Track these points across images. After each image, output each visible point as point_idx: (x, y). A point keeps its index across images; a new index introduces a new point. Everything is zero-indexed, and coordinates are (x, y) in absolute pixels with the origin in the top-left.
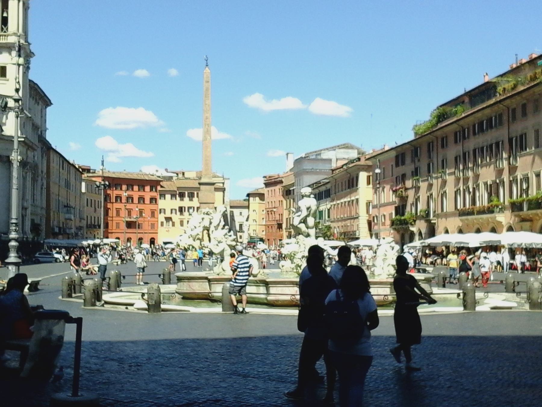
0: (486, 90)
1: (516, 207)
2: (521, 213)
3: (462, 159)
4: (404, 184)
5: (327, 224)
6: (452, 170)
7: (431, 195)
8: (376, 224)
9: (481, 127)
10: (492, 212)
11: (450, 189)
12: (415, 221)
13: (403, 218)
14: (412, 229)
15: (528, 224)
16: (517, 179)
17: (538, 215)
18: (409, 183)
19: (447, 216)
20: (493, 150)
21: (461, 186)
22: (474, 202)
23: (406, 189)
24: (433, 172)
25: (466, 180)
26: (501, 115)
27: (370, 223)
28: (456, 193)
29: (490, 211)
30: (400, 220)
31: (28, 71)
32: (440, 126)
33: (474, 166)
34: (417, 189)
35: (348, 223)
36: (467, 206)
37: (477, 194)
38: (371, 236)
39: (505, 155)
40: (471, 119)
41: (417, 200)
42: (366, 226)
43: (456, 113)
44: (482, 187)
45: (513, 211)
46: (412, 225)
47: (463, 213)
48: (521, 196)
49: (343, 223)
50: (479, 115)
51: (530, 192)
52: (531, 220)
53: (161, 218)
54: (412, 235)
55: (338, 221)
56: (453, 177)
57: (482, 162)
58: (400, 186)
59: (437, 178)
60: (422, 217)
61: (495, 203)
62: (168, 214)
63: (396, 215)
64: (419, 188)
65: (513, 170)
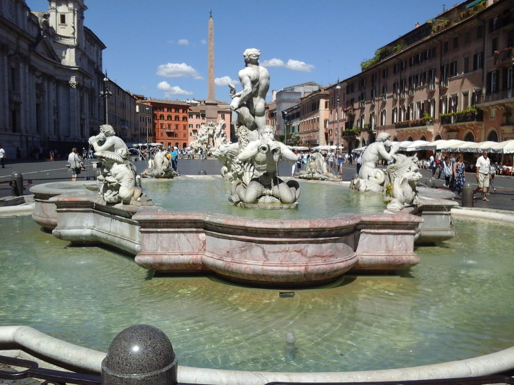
0: (426, 28)
1: (445, 120)
2: (450, 125)
3: (399, 86)
4: (353, 106)
5: (297, 135)
6: (391, 94)
7: (374, 113)
8: (331, 135)
9: (416, 60)
10: (424, 124)
11: (389, 108)
12: (360, 133)
13: (351, 130)
14: (357, 138)
15: (455, 133)
16: (447, 99)
17: (465, 126)
18: (356, 105)
19: (385, 128)
20: (427, 78)
21: (398, 106)
22: (407, 117)
23: (354, 110)
24: (375, 96)
25: (402, 101)
26: (434, 49)
27: (326, 135)
28: (393, 111)
29: (422, 123)
30: (349, 132)
32: (382, 61)
33: (409, 90)
34: (362, 109)
35: (311, 134)
36: (402, 120)
37: (411, 112)
38: (327, 144)
39: (437, 80)
40: (409, 53)
41: (362, 117)
42: (324, 136)
43: (396, 50)
44: (415, 105)
45: (442, 123)
46: (357, 135)
47: (398, 126)
48: (450, 112)
49: (308, 134)
50: (416, 49)
51: (457, 108)
52: (457, 130)
53: (190, 130)
54: (358, 142)
55: (305, 133)
56: (391, 99)
57: (416, 86)
58: (350, 107)
59: (378, 101)
60: (365, 130)
61: (426, 117)
62: (195, 128)
63: (346, 128)
64: (364, 108)
65: (443, 91)
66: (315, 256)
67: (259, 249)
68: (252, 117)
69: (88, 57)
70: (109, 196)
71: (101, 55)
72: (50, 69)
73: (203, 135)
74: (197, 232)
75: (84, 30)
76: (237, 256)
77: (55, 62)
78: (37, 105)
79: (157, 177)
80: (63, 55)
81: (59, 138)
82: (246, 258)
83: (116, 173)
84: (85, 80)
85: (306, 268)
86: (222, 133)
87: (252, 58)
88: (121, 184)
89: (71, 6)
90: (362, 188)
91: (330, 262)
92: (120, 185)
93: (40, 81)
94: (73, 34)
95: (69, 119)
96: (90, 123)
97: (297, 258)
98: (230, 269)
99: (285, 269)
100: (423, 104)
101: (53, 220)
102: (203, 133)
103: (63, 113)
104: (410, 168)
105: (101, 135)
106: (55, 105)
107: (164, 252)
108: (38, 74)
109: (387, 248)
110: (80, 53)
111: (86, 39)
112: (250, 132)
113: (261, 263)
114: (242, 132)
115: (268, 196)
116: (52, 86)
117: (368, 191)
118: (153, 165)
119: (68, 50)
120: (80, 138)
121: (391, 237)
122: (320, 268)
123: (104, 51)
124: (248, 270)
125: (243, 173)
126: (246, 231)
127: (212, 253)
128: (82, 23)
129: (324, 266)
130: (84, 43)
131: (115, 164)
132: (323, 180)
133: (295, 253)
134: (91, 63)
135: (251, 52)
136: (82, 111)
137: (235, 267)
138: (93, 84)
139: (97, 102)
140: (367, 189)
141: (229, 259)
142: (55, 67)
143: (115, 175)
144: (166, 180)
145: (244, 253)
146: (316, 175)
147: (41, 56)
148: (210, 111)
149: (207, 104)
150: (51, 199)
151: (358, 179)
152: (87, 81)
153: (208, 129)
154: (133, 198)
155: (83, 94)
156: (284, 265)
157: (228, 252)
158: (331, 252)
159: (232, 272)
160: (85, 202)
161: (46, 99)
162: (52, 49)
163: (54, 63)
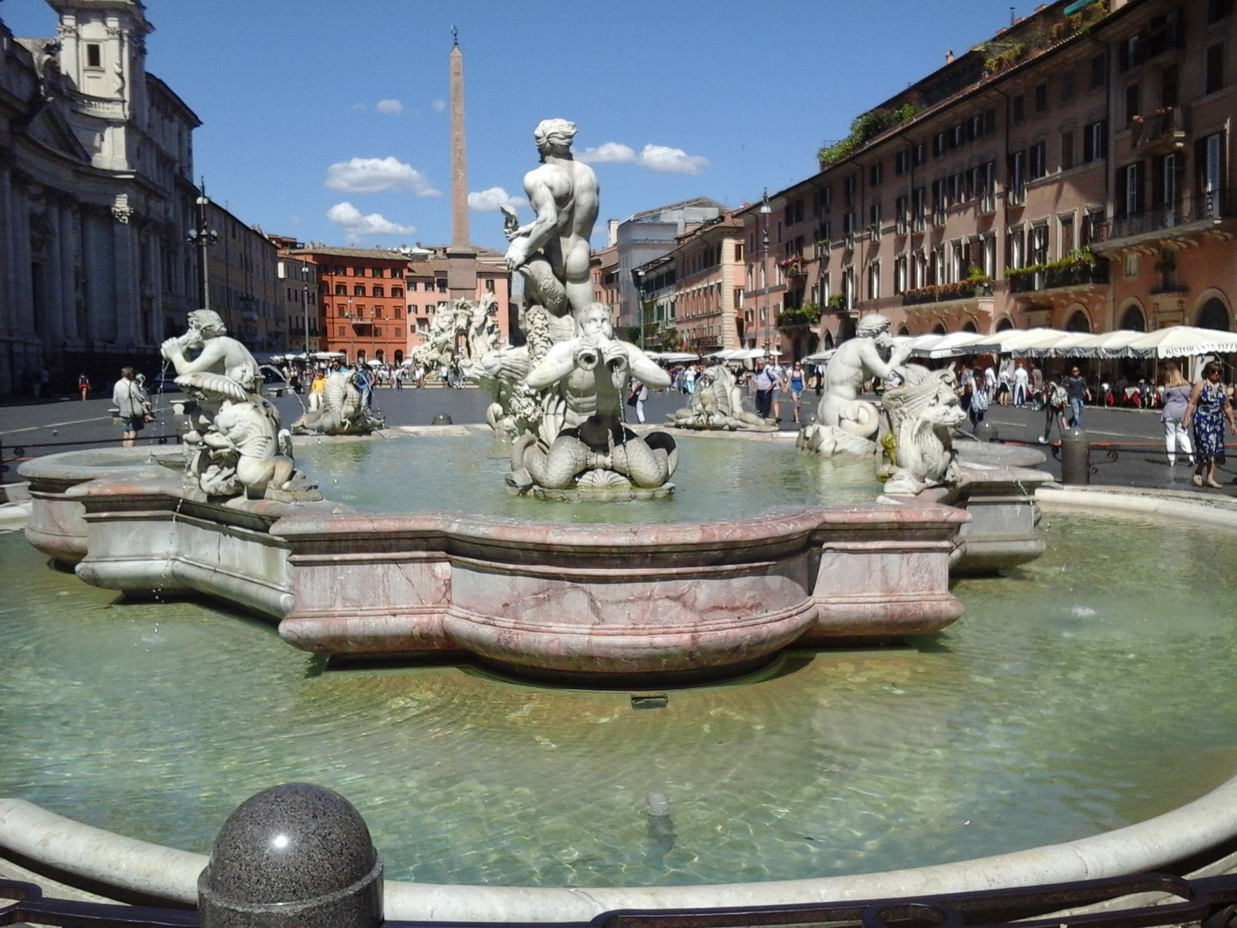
0: (970, 64)
1: (1019, 283)
2: (1031, 294)
3: (911, 203)
4: (801, 254)
5: (671, 326)
6: (891, 223)
7: (851, 269)
8: (752, 324)
9: (949, 141)
10: (971, 294)
11: (886, 258)
12: (819, 317)
13: (798, 312)
14: (814, 330)
15: (1043, 314)
16: (1022, 232)
17: (1066, 296)
18: (809, 252)
19: (877, 306)
20: (974, 183)
21: (907, 251)
22: (931, 277)
23: (805, 263)
24: (855, 229)
25: (917, 239)
26: (991, 114)
27: (740, 324)
28: (897, 263)
29: (967, 292)
30: (794, 317)
31: (143, 57)
32: (868, 144)
33: (933, 213)
34: (824, 261)
35: (704, 323)
36: (919, 286)
37: (939, 265)
38: (742, 345)
39: (998, 188)
40: (931, 125)
41: (824, 280)
42: (734, 327)
43: (901, 118)
44: (949, 249)
45: (1013, 291)
46: (814, 323)
47: (910, 299)
48: (1030, 263)
49: (696, 325)
50: (948, 115)
51: (1048, 254)
52: (1049, 307)
53: (411, 319)
54: (814, 340)
55: (688, 320)
56: (892, 236)
57: (950, 203)
58: (794, 257)
59: (861, 240)
60: (832, 310)
61: (976, 276)
62: (422, 313)
63: (786, 307)
64: (828, 259)
65: (1013, 214)
66: (715, 608)
67: (581, 595)
68: (558, 283)
69: (158, 146)
70: (213, 480)
71: (190, 142)
72: (65, 179)
73: (442, 330)
74: (429, 560)
75: (148, 83)
76: (527, 616)
77: (76, 160)
78: (35, 266)
79: (332, 432)
80: (97, 144)
81: (91, 345)
82: (549, 617)
83: (230, 424)
84: (152, 203)
85: (693, 638)
86: (489, 323)
87: (556, 141)
88: (241, 450)
89: (113, 23)
90: (826, 446)
91: (750, 622)
92: (240, 454)
93: (39, 208)
94: (121, 91)
95: (114, 299)
96: (165, 308)
97: (673, 613)
98: (512, 646)
99: (644, 640)
100: (967, 246)
101: (77, 542)
102: (443, 325)
103: (98, 286)
104: (937, 398)
105: (192, 335)
106: (79, 265)
107: (350, 609)
108: (33, 190)
109: (887, 583)
110: (138, 137)
111: (152, 102)
112: (555, 320)
113: (585, 628)
114: (536, 321)
115: (600, 471)
116: (70, 220)
117: (841, 452)
118: (322, 404)
119: (109, 132)
120: (142, 345)
121: (894, 558)
122: (726, 637)
123: (196, 132)
124: (554, 646)
125: (540, 418)
126: (548, 553)
127: (468, 608)
128: (142, 65)
129: (737, 630)
130: (146, 114)
131: (227, 405)
132: (732, 429)
133: (668, 603)
134: (165, 161)
135: (554, 127)
136: (144, 278)
137: (522, 639)
138: (171, 214)
139: (181, 257)
140: (838, 449)
141: (509, 622)
142: (76, 172)
143: (228, 429)
144: (354, 438)
145: (546, 606)
146: (717, 419)
147: (42, 148)
148: (458, 273)
149: (450, 256)
150: (72, 491)
151: (816, 426)
152: (157, 207)
153: (456, 316)
154: (271, 484)
155: (148, 238)
156: (641, 632)
157: (506, 605)
158: (753, 597)
159: (515, 652)
160: (154, 495)
161: (57, 251)
162: (70, 131)
163: (74, 163)
